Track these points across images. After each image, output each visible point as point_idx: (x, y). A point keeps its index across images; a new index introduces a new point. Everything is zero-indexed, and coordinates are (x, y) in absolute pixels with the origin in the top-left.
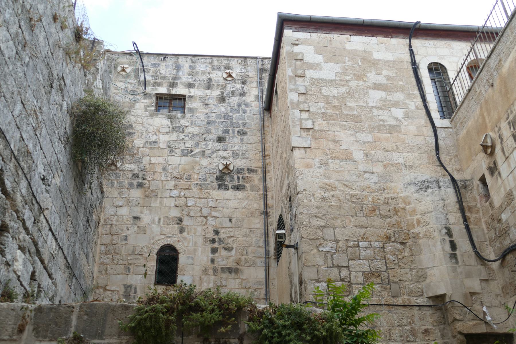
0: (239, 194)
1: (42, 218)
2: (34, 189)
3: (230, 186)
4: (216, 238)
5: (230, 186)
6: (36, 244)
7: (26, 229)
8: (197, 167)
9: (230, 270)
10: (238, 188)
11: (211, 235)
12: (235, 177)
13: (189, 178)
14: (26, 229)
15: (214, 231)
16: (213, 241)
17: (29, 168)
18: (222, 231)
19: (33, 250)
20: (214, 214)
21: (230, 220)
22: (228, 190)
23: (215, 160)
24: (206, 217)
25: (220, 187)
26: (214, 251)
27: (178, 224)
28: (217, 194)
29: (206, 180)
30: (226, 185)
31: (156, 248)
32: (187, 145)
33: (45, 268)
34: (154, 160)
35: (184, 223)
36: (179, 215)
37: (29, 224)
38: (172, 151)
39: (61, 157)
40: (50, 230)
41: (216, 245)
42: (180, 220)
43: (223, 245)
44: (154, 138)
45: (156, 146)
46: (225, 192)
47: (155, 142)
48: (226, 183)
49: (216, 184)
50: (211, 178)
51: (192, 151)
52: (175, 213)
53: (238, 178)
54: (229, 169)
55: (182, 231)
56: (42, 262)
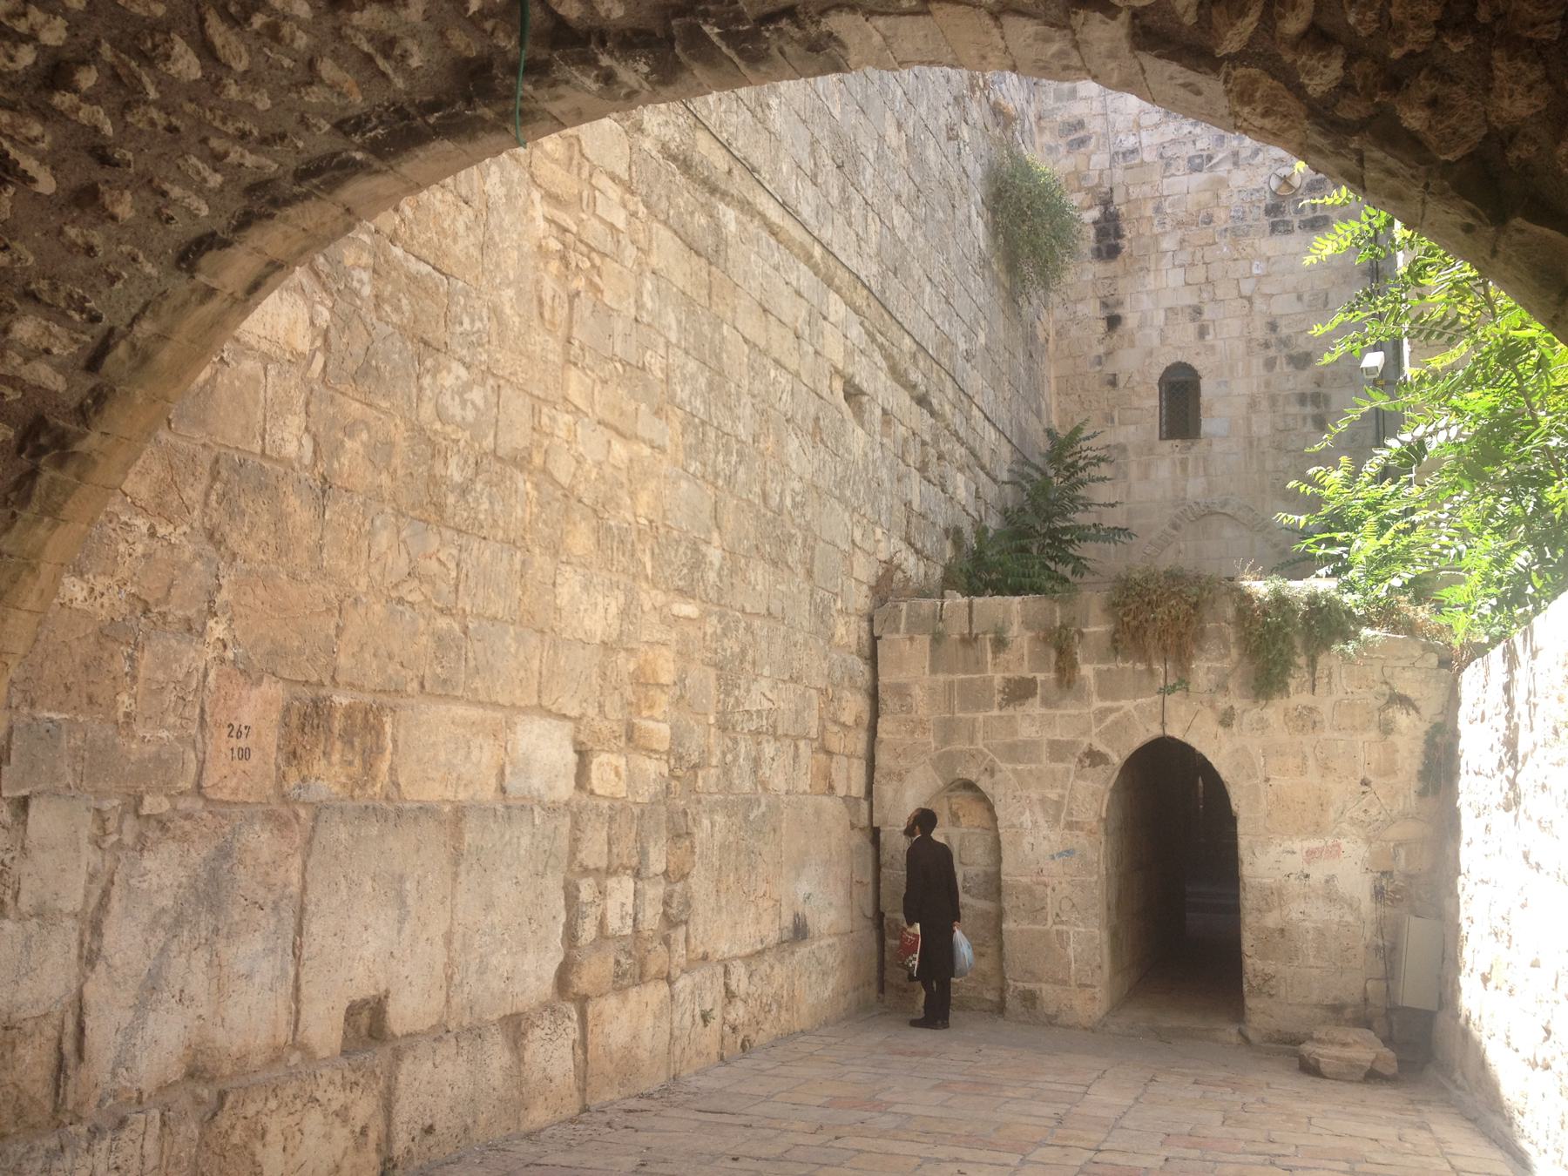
1: (975, 412)
2: (959, 380)
4: (1273, 338)
5: (1296, 225)
6: (973, 453)
7: (959, 439)
8: (1224, 194)
11: (1260, 333)
13: (1209, 220)
14: (959, 439)
16: (1267, 345)
17: (950, 359)
18: (1282, 323)
19: (972, 461)
20: (1267, 289)
21: (1300, 298)
22: (1289, 232)
23: (1264, 170)
24: (1249, 299)
25: (1274, 228)
26: (1270, 364)
27: (1193, 320)
28: (1270, 245)
30: (1286, 223)
31: (1157, 373)
32: (1199, 145)
33: (988, 474)
34: (1135, 192)
35: (1206, 316)
36: (1195, 301)
37: (962, 433)
38: (1168, 165)
39: (980, 300)
40: (986, 417)
41: (1272, 352)
42: (1197, 311)
44: (1130, 142)
45: (1137, 161)
46: (1285, 238)
47: (1132, 152)
48: (1287, 218)
49: (1266, 222)
50: (1255, 210)
51: (1210, 158)
54: (1291, 187)
55: (1202, 332)
56: (983, 468)
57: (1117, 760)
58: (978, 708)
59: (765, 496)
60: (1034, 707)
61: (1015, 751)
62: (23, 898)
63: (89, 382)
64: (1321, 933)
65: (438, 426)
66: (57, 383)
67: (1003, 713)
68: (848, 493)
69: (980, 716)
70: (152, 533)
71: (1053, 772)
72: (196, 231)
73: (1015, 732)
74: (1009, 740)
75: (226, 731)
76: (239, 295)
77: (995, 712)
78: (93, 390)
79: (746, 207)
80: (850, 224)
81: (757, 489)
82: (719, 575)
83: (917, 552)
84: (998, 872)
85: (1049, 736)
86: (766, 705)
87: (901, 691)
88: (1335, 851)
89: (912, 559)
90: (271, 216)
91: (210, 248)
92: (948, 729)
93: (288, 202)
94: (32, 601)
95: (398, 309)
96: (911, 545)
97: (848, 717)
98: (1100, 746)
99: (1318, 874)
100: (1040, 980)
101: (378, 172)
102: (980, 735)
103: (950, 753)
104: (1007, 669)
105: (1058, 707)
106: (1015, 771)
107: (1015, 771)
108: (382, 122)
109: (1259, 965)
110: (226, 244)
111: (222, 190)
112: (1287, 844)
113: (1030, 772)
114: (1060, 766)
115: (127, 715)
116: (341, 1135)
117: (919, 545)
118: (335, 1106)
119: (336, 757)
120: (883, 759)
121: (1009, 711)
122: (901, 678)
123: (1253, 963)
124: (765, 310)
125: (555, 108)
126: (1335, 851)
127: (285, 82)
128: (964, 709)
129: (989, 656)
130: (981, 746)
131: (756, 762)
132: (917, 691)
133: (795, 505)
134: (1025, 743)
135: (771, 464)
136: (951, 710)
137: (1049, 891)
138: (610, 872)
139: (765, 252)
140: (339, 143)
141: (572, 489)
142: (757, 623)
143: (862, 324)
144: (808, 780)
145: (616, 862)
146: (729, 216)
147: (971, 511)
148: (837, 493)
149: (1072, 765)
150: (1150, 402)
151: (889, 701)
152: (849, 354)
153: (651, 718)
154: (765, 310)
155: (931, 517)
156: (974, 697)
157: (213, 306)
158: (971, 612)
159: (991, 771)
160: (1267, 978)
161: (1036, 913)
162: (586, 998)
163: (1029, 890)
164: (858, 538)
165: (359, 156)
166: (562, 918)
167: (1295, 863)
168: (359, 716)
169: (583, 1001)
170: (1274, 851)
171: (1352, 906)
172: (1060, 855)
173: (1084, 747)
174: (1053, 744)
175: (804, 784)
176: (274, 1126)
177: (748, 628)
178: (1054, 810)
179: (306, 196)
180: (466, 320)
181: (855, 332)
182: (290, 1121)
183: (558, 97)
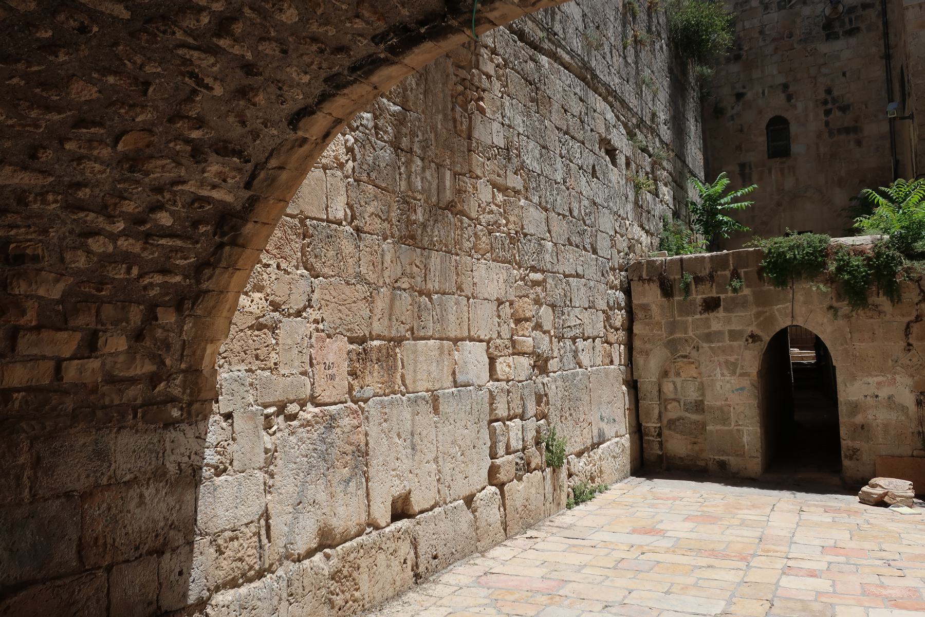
0: (853, 41)
3: (841, 33)
5: (841, 33)
9: (847, 130)
10: (851, 32)
11: (822, 95)
12: (847, 20)
15: (826, 91)
16: (825, 102)
21: (844, 74)
26: (828, 113)
28: (825, 48)
29: (810, 33)
34: (747, 24)
41: (829, 106)
43: (837, 105)
49: (823, 33)
52: (781, 80)
53: (850, 20)
57: (767, 338)
58: (688, 315)
59: (571, 211)
60: (721, 313)
61: (709, 337)
62: (235, 463)
63: (247, 194)
64: (886, 426)
65: (410, 193)
66: (229, 198)
67: (703, 316)
68: (611, 204)
69: (690, 319)
70: (278, 267)
71: (731, 346)
72: (297, 107)
73: (709, 327)
74: (707, 331)
75: (323, 366)
76: (319, 141)
77: (698, 316)
78: (248, 199)
79: (553, 56)
80: (604, 58)
81: (566, 208)
82: (552, 256)
83: (647, 232)
84: (702, 401)
85: (727, 328)
86: (579, 322)
87: (645, 308)
88: (893, 382)
89: (644, 235)
90: (334, 95)
91: (304, 116)
92: (673, 327)
93: (345, 87)
94: (225, 314)
95: (386, 132)
96: (643, 229)
97: (618, 324)
98: (757, 332)
99: (883, 393)
100: (728, 455)
101: (393, 63)
102: (690, 329)
103: (673, 340)
104: (704, 293)
105: (733, 312)
106: (710, 347)
107: (710, 347)
108: (396, 35)
109: (850, 443)
110: (313, 113)
111: (309, 83)
112: (866, 379)
113: (719, 347)
114: (735, 343)
115: (275, 364)
116: (396, 564)
117: (647, 228)
118: (391, 550)
119: (375, 374)
120: (637, 344)
121: (705, 316)
122: (644, 301)
123: (846, 442)
124: (566, 111)
125: (492, 16)
126: (893, 382)
127: (343, 18)
128: (680, 315)
129: (693, 287)
130: (691, 334)
131: (576, 352)
132: (654, 307)
133: (586, 214)
134: (715, 332)
135: (573, 193)
136: (673, 317)
137: (732, 409)
138: (510, 419)
139: (564, 78)
140: (372, 49)
141: (477, 219)
142: (571, 279)
143: (613, 111)
144: (600, 359)
145: (512, 413)
146: (544, 60)
147: (672, 206)
148: (606, 205)
149: (742, 343)
150: (761, 140)
151: (639, 314)
152: (607, 129)
153: (523, 336)
154: (566, 111)
155: (652, 213)
156: (686, 310)
157: (306, 147)
158: (682, 264)
159: (697, 348)
160: (855, 451)
161: (725, 421)
162: (503, 484)
163: (721, 409)
164: (617, 229)
165: (382, 56)
166: (489, 444)
167: (872, 390)
168: (384, 351)
169: (501, 486)
170: (858, 384)
171: (904, 409)
172: (737, 390)
173: (749, 333)
174: (730, 332)
175: (599, 360)
176: (364, 563)
177: (568, 283)
178: (732, 367)
179: (354, 81)
180: (420, 134)
181: (610, 116)
182: (371, 560)
183: (495, 9)
